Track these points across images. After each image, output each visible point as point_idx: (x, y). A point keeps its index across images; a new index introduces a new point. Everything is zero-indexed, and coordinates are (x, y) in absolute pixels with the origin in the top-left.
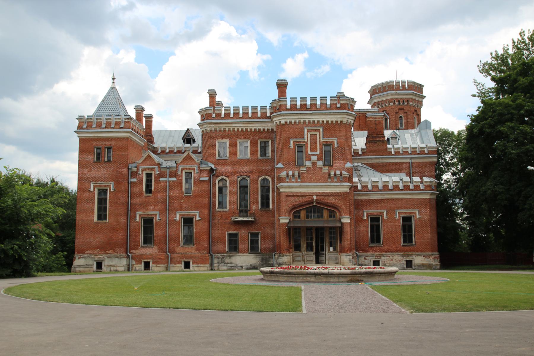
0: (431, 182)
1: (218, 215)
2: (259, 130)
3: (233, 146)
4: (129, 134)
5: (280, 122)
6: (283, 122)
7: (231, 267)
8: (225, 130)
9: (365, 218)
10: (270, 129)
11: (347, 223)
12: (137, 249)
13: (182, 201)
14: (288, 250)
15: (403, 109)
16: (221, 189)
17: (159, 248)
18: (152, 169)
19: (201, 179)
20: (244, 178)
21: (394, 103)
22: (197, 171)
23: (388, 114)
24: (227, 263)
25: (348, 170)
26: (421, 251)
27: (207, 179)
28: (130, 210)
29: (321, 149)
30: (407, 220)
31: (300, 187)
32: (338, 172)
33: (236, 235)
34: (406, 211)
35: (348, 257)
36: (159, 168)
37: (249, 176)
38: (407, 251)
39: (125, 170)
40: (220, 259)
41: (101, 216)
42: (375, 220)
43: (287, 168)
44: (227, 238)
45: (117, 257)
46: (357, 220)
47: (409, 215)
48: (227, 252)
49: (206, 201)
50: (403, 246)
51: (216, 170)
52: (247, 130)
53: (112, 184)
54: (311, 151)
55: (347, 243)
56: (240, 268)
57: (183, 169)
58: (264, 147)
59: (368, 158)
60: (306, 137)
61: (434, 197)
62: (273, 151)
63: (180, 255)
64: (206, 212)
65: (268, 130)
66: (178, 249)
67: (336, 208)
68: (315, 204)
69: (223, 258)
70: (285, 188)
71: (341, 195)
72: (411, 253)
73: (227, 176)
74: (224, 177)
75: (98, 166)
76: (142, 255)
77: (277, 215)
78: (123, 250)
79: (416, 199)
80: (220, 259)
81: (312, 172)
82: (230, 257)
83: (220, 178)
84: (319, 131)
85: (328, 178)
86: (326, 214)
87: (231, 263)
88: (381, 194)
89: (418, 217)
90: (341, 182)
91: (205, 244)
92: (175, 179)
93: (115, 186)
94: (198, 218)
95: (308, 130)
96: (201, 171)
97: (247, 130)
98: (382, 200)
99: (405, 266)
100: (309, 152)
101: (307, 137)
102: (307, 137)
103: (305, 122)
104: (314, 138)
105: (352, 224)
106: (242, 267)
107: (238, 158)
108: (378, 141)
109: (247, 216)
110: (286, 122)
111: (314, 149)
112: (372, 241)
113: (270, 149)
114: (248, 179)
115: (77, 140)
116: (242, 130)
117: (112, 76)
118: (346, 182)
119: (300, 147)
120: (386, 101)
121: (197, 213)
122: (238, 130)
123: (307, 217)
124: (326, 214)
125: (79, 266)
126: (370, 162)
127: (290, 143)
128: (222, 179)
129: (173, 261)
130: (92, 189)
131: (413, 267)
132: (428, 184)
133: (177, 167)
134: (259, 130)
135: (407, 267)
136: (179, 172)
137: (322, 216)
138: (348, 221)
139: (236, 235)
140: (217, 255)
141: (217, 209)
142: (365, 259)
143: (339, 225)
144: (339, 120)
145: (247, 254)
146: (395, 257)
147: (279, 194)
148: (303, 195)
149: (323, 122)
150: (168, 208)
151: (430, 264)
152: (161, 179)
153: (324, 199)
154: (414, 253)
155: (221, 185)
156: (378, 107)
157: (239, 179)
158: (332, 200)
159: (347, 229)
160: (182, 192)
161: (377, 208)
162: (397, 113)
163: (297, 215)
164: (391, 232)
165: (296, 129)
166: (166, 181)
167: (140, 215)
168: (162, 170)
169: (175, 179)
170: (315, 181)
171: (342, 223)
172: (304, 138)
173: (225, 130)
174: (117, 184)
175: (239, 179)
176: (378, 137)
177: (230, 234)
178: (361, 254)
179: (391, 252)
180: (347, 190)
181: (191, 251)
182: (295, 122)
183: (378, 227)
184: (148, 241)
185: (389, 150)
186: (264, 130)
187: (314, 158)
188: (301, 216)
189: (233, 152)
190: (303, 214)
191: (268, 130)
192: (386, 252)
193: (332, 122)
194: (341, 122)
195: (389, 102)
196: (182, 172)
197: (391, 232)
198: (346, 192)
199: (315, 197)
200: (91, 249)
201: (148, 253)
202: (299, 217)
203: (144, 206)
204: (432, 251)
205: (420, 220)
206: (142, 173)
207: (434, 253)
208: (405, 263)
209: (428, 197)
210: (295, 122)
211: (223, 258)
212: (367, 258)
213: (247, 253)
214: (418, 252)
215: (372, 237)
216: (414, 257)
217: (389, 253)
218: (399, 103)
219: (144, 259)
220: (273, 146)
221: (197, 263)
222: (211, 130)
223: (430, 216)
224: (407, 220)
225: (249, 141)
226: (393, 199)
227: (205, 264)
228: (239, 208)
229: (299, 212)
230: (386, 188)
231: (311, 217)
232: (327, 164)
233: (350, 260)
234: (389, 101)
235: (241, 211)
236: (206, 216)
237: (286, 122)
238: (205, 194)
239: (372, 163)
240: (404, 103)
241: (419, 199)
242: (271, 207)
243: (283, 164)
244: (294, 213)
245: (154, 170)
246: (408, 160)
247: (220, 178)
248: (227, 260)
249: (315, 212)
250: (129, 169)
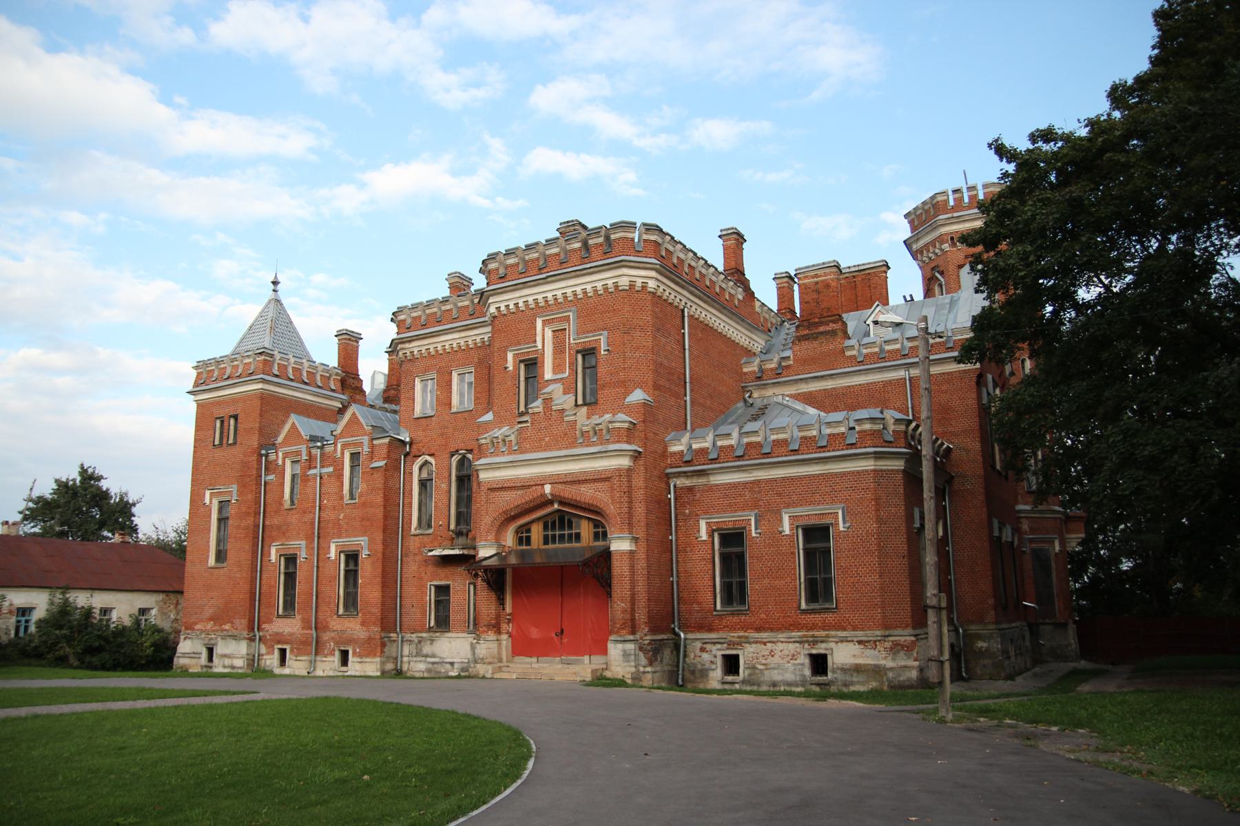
0: (872, 420)
1: (413, 544)
4: (260, 386)
7: (433, 663)
11: (622, 553)
12: (270, 621)
14: (496, 628)
16: (423, 484)
17: (303, 620)
19: (374, 465)
22: (366, 449)
23: (942, 273)
24: (427, 656)
25: (628, 409)
26: (854, 629)
27: (382, 463)
28: (258, 539)
29: (573, 364)
30: (816, 534)
31: (513, 464)
33: (447, 588)
34: (811, 513)
35: (620, 646)
38: (813, 627)
39: (254, 458)
40: (413, 646)
41: (221, 556)
42: (733, 539)
43: (499, 422)
44: (431, 595)
45: (234, 637)
47: (823, 521)
48: (430, 629)
49: (379, 513)
50: (805, 612)
51: (411, 444)
53: (234, 488)
54: (554, 372)
55: (619, 606)
56: (448, 666)
57: (345, 446)
59: (796, 381)
60: (539, 339)
61: (899, 464)
63: (333, 634)
64: (379, 537)
66: (335, 624)
68: (556, 506)
69: (420, 642)
71: (607, 479)
72: (823, 633)
74: (428, 458)
75: (219, 453)
76: (277, 634)
78: (245, 622)
79: (836, 474)
80: (413, 646)
81: (543, 425)
82: (432, 641)
84: (567, 319)
85: (569, 437)
87: (434, 656)
88: (740, 469)
90: (608, 442)
91: (376, 611)
92: (331, 469)
93: (240, 493)
95: (545, 323)
96: (372, 447)
99: (807, 672)
101: (544, 339)
102: (544, 339)
105: (641, 555)
106: (452, 664)
107: (454, 410)
108: (822, 333)
111: (557, 368)
112: (728, 599)
114: (470, 456)
115: (195, 405)
117: (272, 279)
118: (618, 442)
119: (532, 365)
120: (933, 243)
123: (546, 542)
124: (585, 530)
125: (184, 655)
126: (805, 388)
128: (426, 462)
129: (319, 648)
130: (207, 501)
131: (830, 675)
132: (867, 426)
133: (335, 444)
135: (1087, 650)
136: (339, 454)
137: (578, 536)
139: (447, 588)
140: (408, 636)
141: (413, 531)
142: (703, 650)
144: (610, 282)
145: (465, 635)
146: (780, 646)
148: (524, 486)
150: (320, 535)
151: (877, 666)
152: (312, 472)
153: (570, 492)
154: (833, 633)
155: (425, 475)
158: (586, 493)
159: (620, 568)
160: (342, 498)
161: (733, 508)
164: (777, 572)
167: (277, 551)
169: (331, 469)
170: (547, 448)
171: (606, 555)
172: (535, 341)
174: (243, 487)
175: (455, 459)
176: (821, 324)
177: (437, 587)
178: (690, 636)
179: (772, 630)
180: (625, 462)
181: (354, 627)
183: (741, 557)
184: (289, 605)
185: (848, 353)
188: (582, 534)
189: (444, 401)
190: (537, 533)
192: (759, 629)
194: (616, 286)
195: (942, 243)
196: (343, 454)
197: (777, 572)
198: (619, 470)
199: (548, 489)
200: (202, 620)
201: (287, 630)
203: (283, 532)
204: (886, 627)
205: (846, 535)
206: (284, 463)
207: (896, 632)
208: (807, 661)
209: (868, 465)
211: (420, 642)
212: (708, 647)
213: (464, 632)
214: (845, 629)
215: (727, 588)
216: (832, 645)
217: (764, 635)
219: (279, 643)
221: (361, 656)
223: (879, 520)
224: (816, 534)
226: (775, 480)
227: (375, 655)
228: (452, 527)
229: (526, 528)
230: (753, 451)
231: (554, 541)
233: (626, 655)
234: (941, 240)
235: (459, 534)
236: (380, 548)
238: (379, 499)
239: (810, 393)
241: (844, 474)
244: (517, 532)
246: (901, 373)
247: (420, 461)
248: (427, 649)
249: (562, 527)
250: (261, 455)
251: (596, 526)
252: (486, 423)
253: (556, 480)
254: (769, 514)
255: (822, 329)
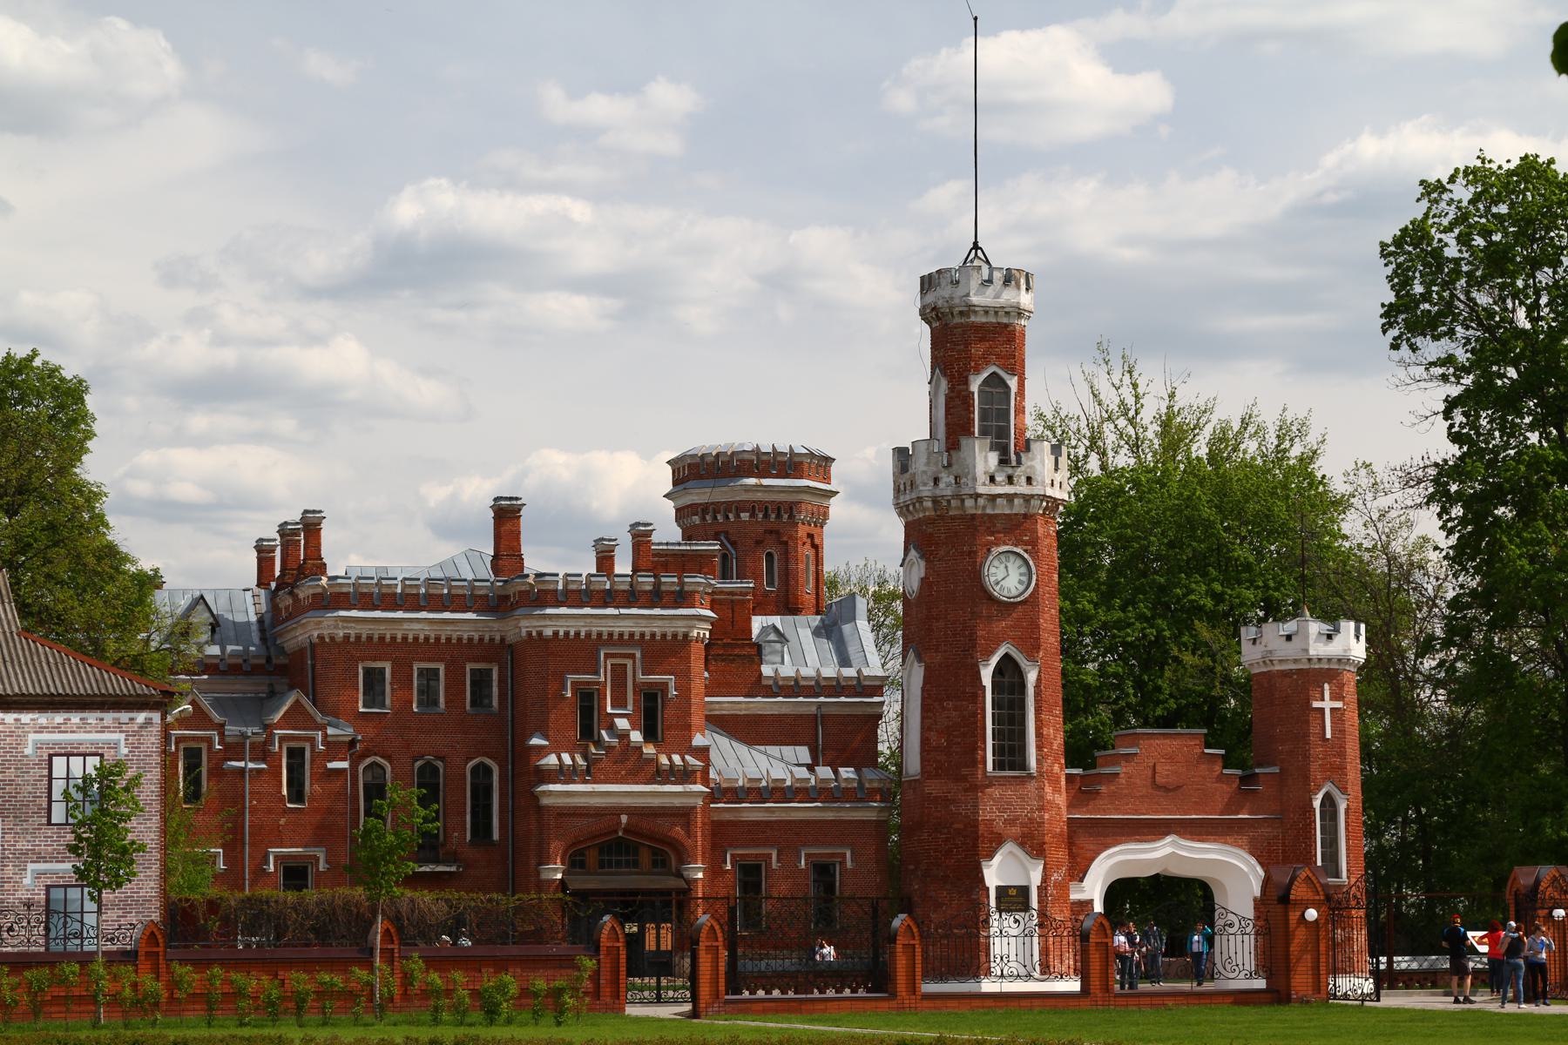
2: (470, 639)
3: (402, 679)
5: (540, 634)
6: (548, 632)
8: (382, 638)
9: (729, 867)
10: (498, 638)
13: (282, 821)
15: (777, 532)
18: (201, 739)
20: (428, 763)
21: (753, 515)
23: (733, 544)
30: (823, 871)
32: (676, 758)
36: (222, 735)
37: (442, 759)
42: (750, 874)
46: (714, 871)
52: (438, 639)
54: (613, 707)
58: (481, 681)
62: (502, 695)
65: (492, 640)
67: (670, 844)
70: (555, 791)
73: (388, 757)
77: (533, 862)
83: (368, 761)
84: (633, 656)
86: (645, 858)
89: (849, 864)
94: (322, 866)
95: (607, 656)
97: (438, 639)
98: (768, 823)
100: (609, 710)
103: (600, 635)
104: (619, 674)
109: (437, 862)
110: (556, 634)
111: (619, 702)
113: (495, 690)
114: (440, 764)
116: (427, 639)
120: (728, 506)
121: (321, 854)
122: (416, 639)
124: (645, 858)
127: (564, 688)
134: (470, 639)
137: (636, 864)
138: (700, 875)
143: (672, 883)
147: (540, 809)
148: (598, 813)
149: (642, 635)
156: (704, 519)
157: (418, 764)
162: (758, 543)
163: (575, 863)
165: (583, 650)
166: (242, 771)
168: (228, 740)
172: (597, 673)
173: (382, 638)
175: (418, 764)
182: (577, 634)
185: (765, 682)
186: (481, 639)
187: (622, 724)
190: (592, 857)
191: (492, 640)
192: (776, 948)
193: (664, 636)
199: (624, 819)
202: (582, 865)
210: (577, 634)
218: (766, 516)
220: (501, 681)
222: (347, 637)
225: (442, 667)
232: (650, 734)
234: (740, 507)
237: (556, 634)
240: (779, 516)
241: (851, 822)
242: (496, 836)
243: (546, 737)
245: (209, 740)
247: (368, 761)
251: (654, 854)
252: (541, 747)
253: (632, 811)
254: (788, 852)
255: (736, 652)
